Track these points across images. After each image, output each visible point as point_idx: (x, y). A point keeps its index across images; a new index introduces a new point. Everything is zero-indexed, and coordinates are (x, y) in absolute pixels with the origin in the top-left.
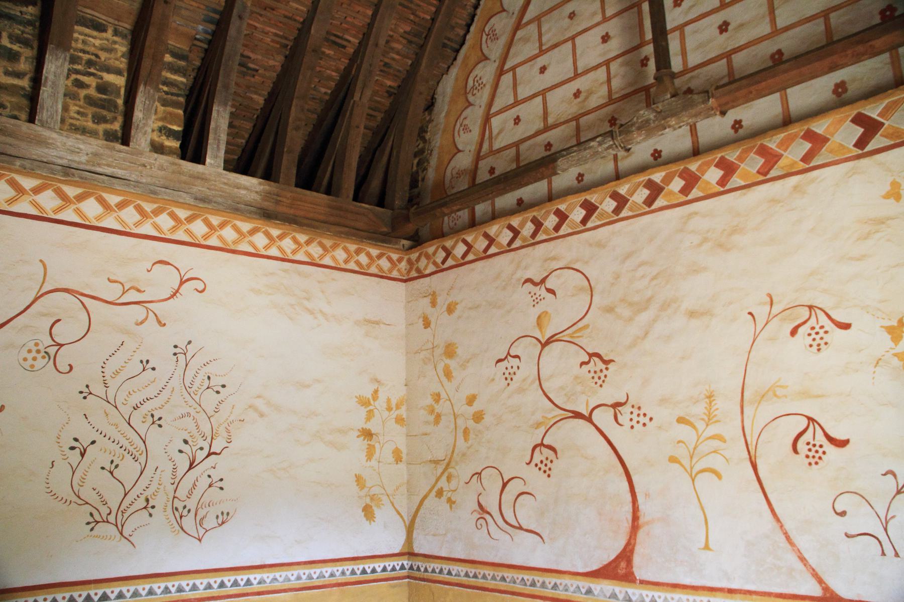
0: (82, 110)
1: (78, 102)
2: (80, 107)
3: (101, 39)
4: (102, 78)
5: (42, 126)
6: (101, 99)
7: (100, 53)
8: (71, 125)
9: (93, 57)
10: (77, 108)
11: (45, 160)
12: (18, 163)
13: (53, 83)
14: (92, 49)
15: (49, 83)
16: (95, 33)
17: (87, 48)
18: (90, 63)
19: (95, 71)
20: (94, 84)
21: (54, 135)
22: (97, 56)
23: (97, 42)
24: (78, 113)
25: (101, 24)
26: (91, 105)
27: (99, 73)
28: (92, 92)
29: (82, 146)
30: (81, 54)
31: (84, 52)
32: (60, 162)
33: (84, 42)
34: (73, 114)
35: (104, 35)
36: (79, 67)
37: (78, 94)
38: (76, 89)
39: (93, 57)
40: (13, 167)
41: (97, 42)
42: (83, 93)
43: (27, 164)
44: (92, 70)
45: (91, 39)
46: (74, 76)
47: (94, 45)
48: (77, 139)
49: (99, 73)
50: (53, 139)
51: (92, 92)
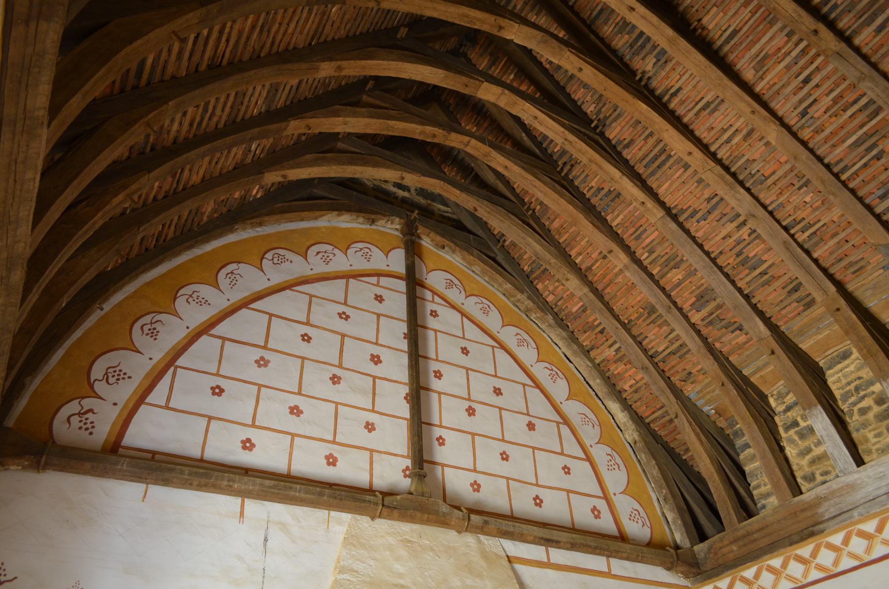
0: (877, 432)
1: (871, 427)
2: (874, 429)
3: (852, 363)
4: (873, 393)
5: (845, 474)
6: (886, 410)
7: (860, 374)
8: (877, 450)
9: (858, 382)
10: (873, 433)
11: (871, 498)
12: (855, 513)
13: (828, 436)
14: (854, 376)
15: (826, 438)
16: (847, 362)
17: (849, 379)
18: (857, 389)
19: (864, 392)
20: (872, 403)
21: (856, 476)
22: (860, 378)
23: (852, 368)
24: (875, 436)
25: (845, 352)
26: (881, 421)
27: (869, 391)
28: (876, 409)
29: (882, 469)
30: (848, 388)
31: (849, 384)
32: (882, 491)
33: (845, 376)
34: (874, 440)
35: (853, 357)
36: (853, 399)
37: (867, 420)
38: (864, 417)
39: (858, 382)
40: (853, 520)
41: (852, 368)
42: (871, 415)
43: (861, 510)
44: (862, 393)
45: (847, 370)
46: (856, 409)
47: (852, 372)
48: (872, 466)
49: (869, 391)
50: (859, 479)
51: (876, 409)
